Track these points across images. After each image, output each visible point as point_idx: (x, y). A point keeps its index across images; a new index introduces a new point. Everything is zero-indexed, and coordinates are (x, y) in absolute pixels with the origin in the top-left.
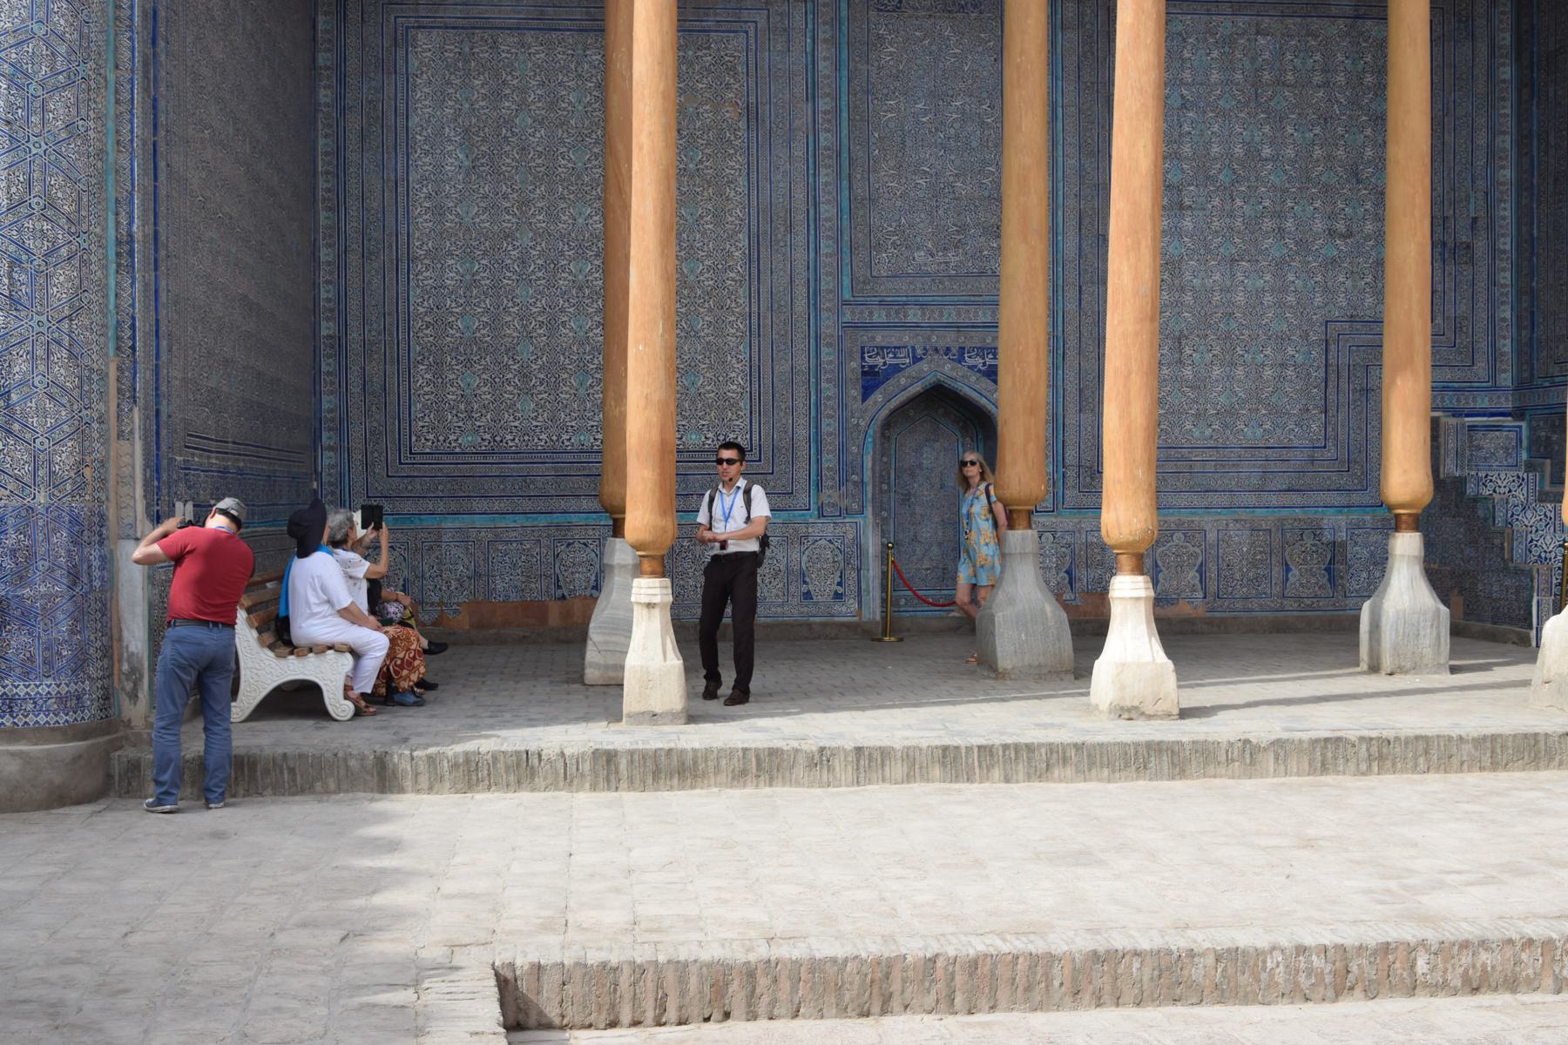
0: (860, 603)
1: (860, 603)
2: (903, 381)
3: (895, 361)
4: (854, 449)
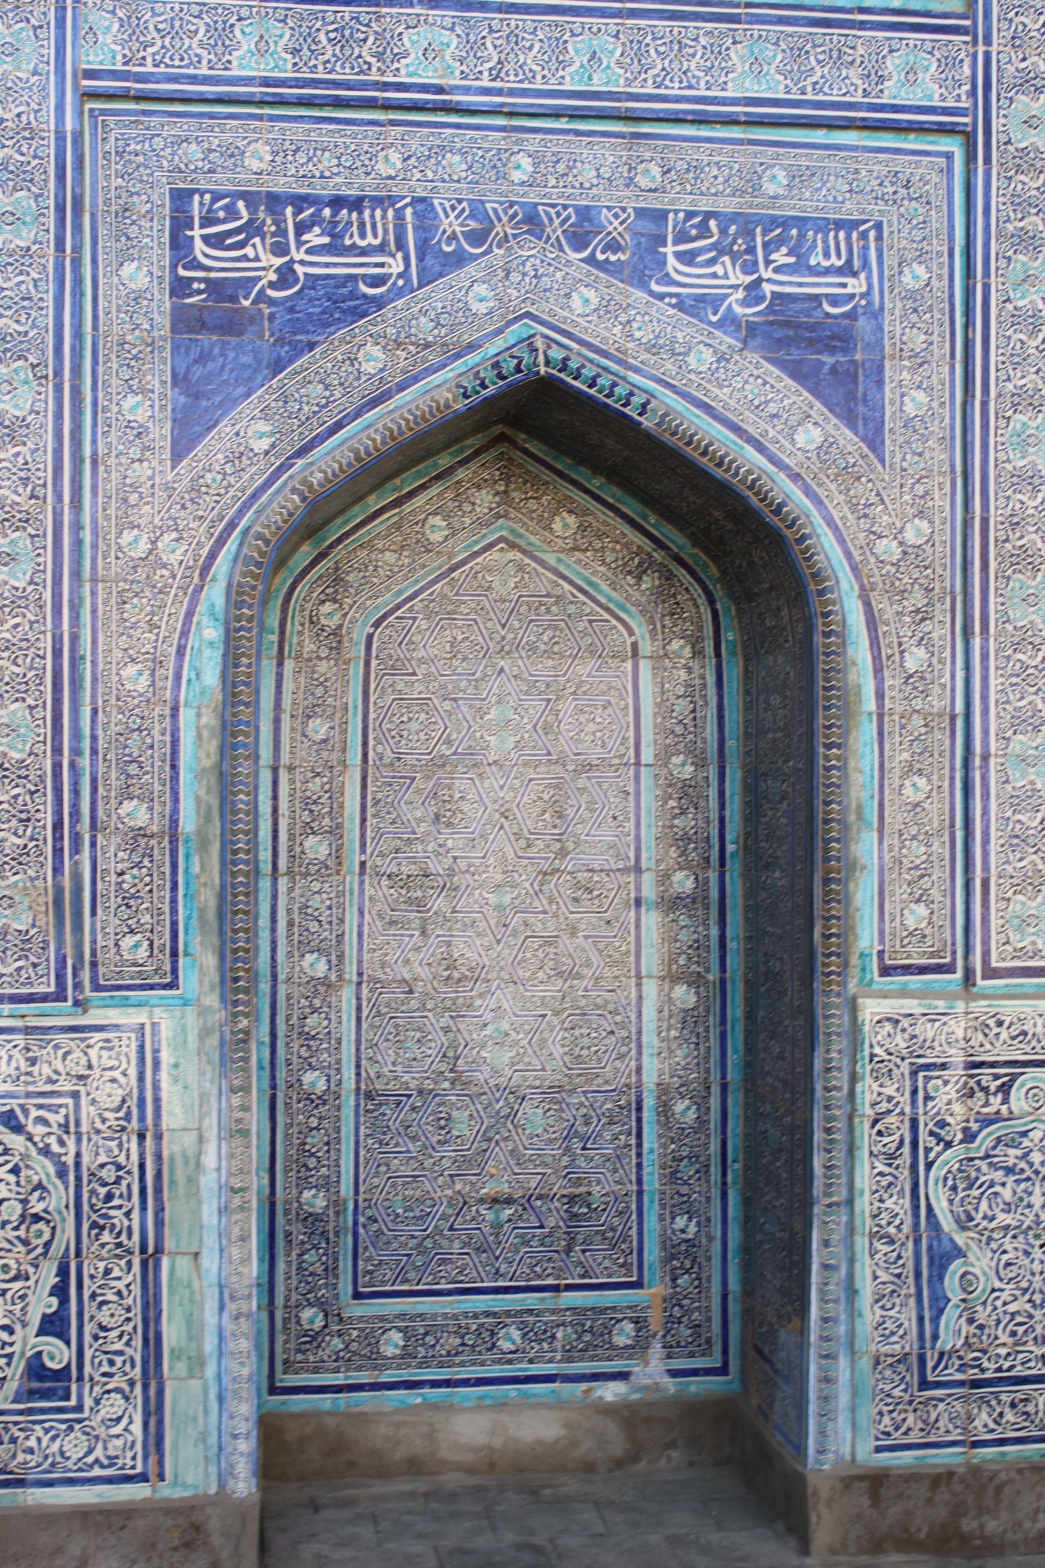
0: (154, 1412)
1: (154, 1412)
2: (373, 359)
3: (339, 266)
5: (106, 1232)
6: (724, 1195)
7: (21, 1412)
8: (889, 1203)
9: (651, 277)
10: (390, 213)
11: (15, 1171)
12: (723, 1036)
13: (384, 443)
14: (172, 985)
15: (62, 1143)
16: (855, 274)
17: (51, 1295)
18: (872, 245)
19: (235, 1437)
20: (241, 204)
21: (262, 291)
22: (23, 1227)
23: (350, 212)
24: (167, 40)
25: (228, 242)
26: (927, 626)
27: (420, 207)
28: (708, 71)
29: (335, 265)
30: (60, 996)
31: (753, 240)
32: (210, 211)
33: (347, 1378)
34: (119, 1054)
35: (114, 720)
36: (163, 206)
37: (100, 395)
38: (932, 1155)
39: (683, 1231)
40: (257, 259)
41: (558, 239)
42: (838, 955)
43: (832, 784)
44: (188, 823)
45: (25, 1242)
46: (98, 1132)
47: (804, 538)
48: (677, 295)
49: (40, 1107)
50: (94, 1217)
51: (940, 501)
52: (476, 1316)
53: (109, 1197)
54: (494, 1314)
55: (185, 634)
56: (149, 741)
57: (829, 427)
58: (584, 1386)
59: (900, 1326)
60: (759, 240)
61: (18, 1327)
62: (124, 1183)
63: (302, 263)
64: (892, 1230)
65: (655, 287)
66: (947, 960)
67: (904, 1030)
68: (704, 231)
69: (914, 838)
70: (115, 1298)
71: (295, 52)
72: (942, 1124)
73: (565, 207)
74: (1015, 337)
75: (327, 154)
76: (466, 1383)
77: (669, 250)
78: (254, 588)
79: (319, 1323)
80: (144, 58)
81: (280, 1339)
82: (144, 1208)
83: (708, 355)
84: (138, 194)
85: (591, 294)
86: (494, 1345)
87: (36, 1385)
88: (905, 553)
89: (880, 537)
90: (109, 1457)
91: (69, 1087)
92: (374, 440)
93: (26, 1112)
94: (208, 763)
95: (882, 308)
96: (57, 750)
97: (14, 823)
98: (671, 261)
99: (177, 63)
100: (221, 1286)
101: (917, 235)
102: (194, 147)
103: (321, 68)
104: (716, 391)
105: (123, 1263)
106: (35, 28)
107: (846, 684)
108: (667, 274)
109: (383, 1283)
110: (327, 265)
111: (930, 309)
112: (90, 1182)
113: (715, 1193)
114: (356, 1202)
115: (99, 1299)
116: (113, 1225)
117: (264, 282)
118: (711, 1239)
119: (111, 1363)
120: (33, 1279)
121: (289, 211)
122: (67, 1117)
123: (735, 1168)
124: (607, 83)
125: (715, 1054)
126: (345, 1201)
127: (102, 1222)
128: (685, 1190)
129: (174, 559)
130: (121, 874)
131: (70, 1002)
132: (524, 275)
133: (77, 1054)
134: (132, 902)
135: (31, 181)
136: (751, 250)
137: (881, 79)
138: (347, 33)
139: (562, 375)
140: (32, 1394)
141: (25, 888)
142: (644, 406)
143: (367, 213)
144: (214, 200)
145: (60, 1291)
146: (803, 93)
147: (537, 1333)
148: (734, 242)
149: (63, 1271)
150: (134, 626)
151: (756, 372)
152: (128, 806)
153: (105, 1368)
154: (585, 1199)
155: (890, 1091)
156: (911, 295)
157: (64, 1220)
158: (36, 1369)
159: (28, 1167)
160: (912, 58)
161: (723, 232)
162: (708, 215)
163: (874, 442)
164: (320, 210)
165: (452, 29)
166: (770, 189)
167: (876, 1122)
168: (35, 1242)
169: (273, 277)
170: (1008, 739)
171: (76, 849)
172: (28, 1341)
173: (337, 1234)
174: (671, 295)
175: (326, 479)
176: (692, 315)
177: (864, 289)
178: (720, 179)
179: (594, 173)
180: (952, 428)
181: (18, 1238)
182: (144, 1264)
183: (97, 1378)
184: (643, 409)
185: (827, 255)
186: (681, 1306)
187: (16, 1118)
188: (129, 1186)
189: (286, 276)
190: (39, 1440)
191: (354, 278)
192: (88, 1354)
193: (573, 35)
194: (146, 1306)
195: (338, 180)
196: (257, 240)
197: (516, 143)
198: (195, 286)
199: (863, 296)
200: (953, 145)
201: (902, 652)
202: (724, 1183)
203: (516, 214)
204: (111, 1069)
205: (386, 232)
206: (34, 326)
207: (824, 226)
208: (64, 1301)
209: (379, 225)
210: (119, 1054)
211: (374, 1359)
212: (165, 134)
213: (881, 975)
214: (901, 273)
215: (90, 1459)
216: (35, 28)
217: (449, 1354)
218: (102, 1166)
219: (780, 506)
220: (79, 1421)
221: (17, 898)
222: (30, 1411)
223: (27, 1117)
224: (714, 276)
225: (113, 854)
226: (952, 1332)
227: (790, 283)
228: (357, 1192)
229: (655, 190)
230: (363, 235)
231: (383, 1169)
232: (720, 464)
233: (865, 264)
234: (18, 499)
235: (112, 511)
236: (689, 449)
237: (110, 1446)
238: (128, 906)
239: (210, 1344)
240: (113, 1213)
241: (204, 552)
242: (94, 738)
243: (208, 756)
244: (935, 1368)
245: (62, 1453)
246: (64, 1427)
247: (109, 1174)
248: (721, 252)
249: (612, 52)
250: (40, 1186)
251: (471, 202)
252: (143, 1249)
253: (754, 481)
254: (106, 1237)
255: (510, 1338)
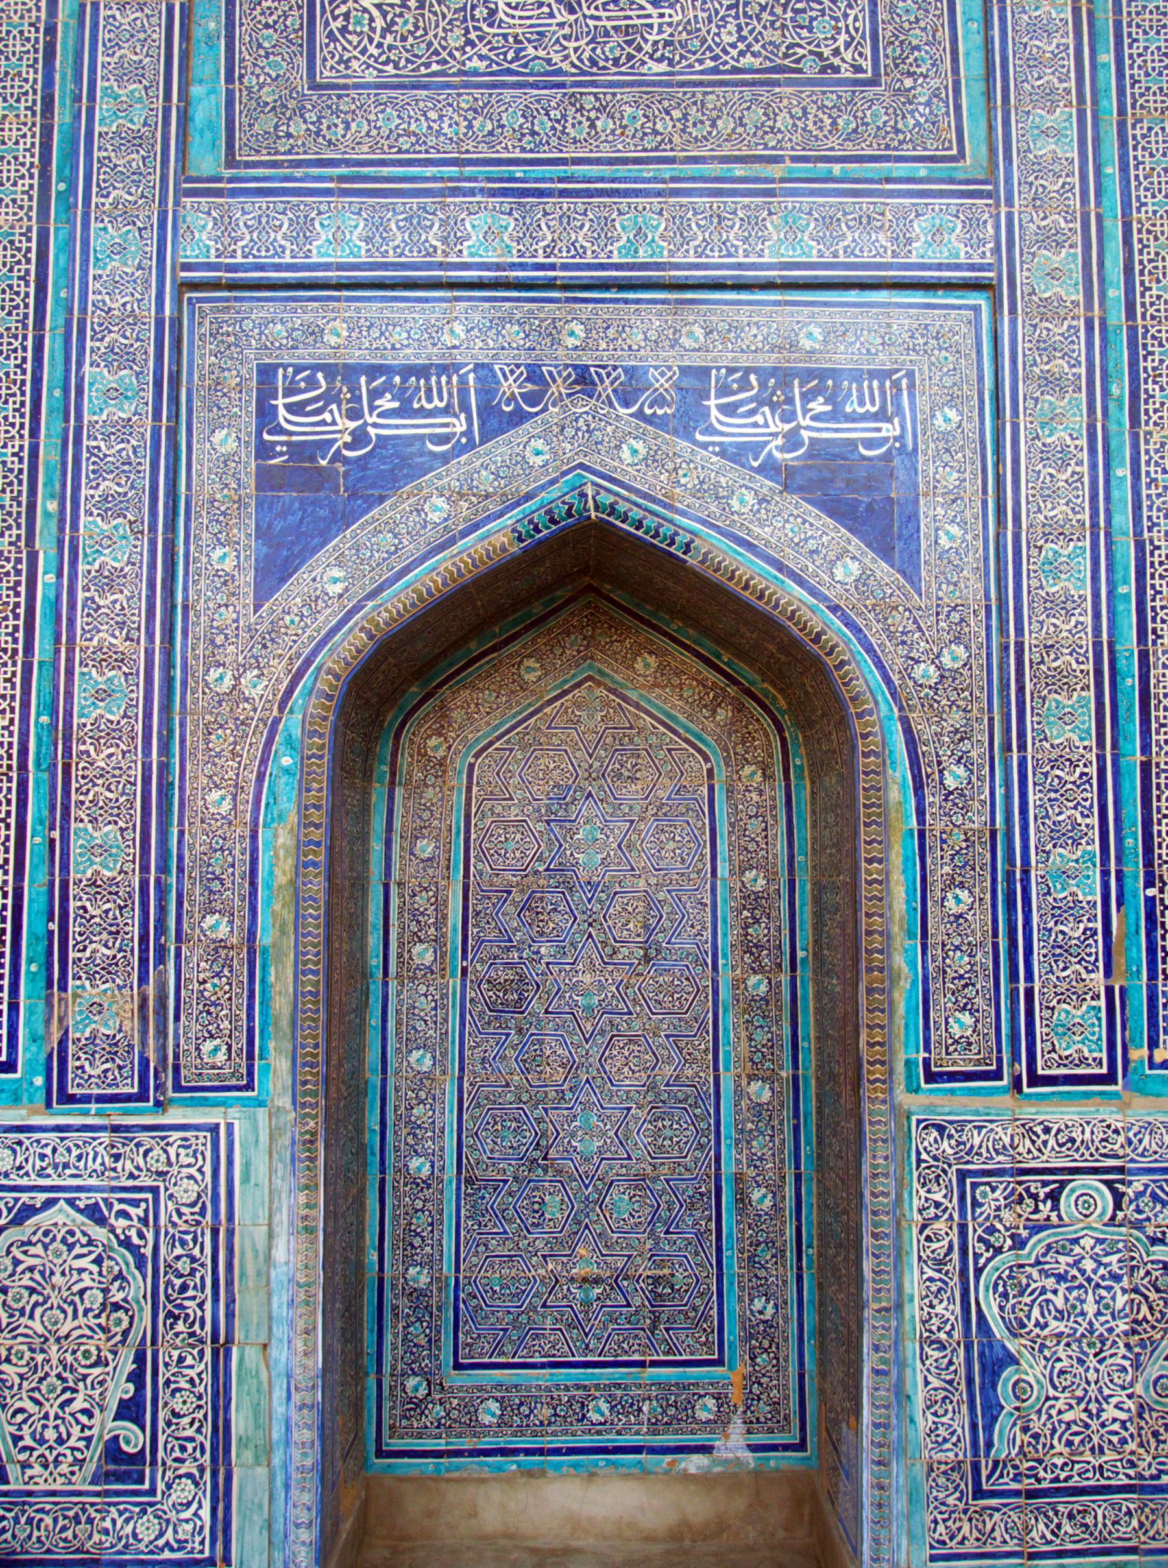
0: (222, 1498)
1: (222, 1498)
2: (438, 509)
3: (405, 427)
4: (218, 801)
5: (181, 1322)
6: (800, 1278)
7: (98, 1494)
8: (939, 1309)
9: (695, 429)
10: (455, 378)
11: (98, 1261)
12: (796, 1128)
13: (445, 584)
14: (249, 1087)
15: (141, 1235)
16: (889, 420)
17: (128, 1381)
18: (905, 393)
19: (297, 1526)
20: (320, 375)
21: (338, 451)
22: (104, 1315)
23: (418, 381)
24: (255, 235)
25: (308, 409)
26: (966, 746)
27: (483, 373)
28: (745, 240)
29: (404, 426)
30: (142, 1096)
31: (792, 391)
32: (292, 382)
33: (447, 1444)
34: (195, 1152)
35: (197, 841)
36: (251, 379)
37: (192, 548)
38: (982, 1261)
39: (761, 1312)
40: (334, 423)
41: (608, 396)
42: (883, 1063)
43: (875, 897)
44: (265, 937)
45: (105, 1330)
46: (174, 1225)
47: (842, 663)
48: (720, 444)
49: (121, 1201)
50: (170, 1307)
51: (976, 626)
52: (567, 1388)
53: (184, 1288)
54: (585, 1388)
55: (264, 761)
56: (230, 859)
57: (867, 561)
58: (668, 1458)
59: (952, 1433)
60: (797, 391)
61: (97, 1411)
62: (198, 1275)
63: (375, 425)
64: (943, 1336)
65: (699, 437)
66: (994, 1067)
67: (950, 1137)
68: (745, 385)
69: (957, 948)
70: (188, 1386)
71: (368, 240)
72: (991, 1230)
73: (615, 368)
74: (1044, 472)
75: (398, 329)
76: (557, 1452)
77: (712, 403)
78: (325, 719)
79: (422, 1392)
80: (235, 251)
81: (387, 1405)
82: (216, 1300)
83: (750, 498)
84: (229, 370)
85: (639, 446)
86: (584, 1416)
87: (111, 1467)
88: (942, 676)
89: (917, 662)
90: (178, 1541)
91: (149, 1182)
92: (435, 582)
93: (110, 1206)
94: (282, 879)
95: (915, 449)
96: (145, 868)
97: (105, 936)
98: (714, 412)
99: (263, 254)
100: (289, 1376)
101: (947, 381)
102: (279, 326)
103: (391, 252)
104: (758, 530)
105: (195, 1352)
106: (140, 229)
107: (887, 802)
108: (711, 425)
109: (481, 1355)
110: (397, 427)
111: (962, 447)
112: (166, 1273)
113: (791, 1277)
114: (457, 1279)
115: (173, 1386)
116: (187, 1315)
117: (340, 443)
118: (786, 1320)
119: (183, 1449)
120: (112, 1365)
121: (363, 379)
122: (146, 1211)
123: (810, 1252)
124: (651, 256)
125: (789, 1145)
126: (447, 1278)
127: (177, 1312)
128: (762, 1273)
129: (255, 693)
130: (205, 982)
131: (151, 1103)
132: (578, 429)
133: (157, 1151)
134: (212, 1009)
135: (134, 361)
136: (790, 401)
137: (909, 241)
138: (415, 221)
139: (611, 519)
140: (109, 1477)
141: (114, 996)
142: (688, 545)
143: (434, 379)
144: (296, 373)
145: (137, 1378)
146: (835, 256)
147: (624, 1407)
148: (773, 394)
149: (140, 1358)
150: (219, 755)
151: (795, 512)
152: (210, 920)
153: (177, 1454)
154: (669, 1281)
155: (938, 1197)
156: (944, 436)
157: (141, 1309)
158: (113, 1451)
159: (110, 1258)
160: (937, 222)
161: (763, 385)
162: (748, 371)
163: (910, 572)
164: (392, 379)
165: (510, 214)
166: (807, 344)
167: (924, 1227)
168: (114, 1330)
169: (348, 439)
170: (1048, 853)
171: (161, 959)
172: (106, 1425)
173: (439, 1309)
174: (714, 444)
175: (392, 618)
176: (735, 462)
177: (898, 433)
178: (760, 337)
179: (641, 336)
180: (986, 559)
181: (99, 1325)
182: (215, 1353)
183: (169, 1463)
184: (687, 548)
185: (861, 403)
186: (760, 1384)
187: (101, 1211)
188: (202, 1278)
189: (359, 438)
190: (114, 1521)
191: (421, 438)
192: (161, 1439)
193: (620, 214)
194: (216, 1394)
195: (408, 351)
196: (334, 407)
197: (569, 313)
198: (278, 448)
199: (896, 439)
200: (980, 300)
201: (941, 772)
202: (800, 1268)
203: (569, 375)
204: (189, 1165)
205: (450, 394)
206: (132, 487)
207: (857, 376)
208: (140, 1387)
209: (445, 390)
210: (195, 1152)
211: (473, 1426)
212: (253, 317)
213: (926, 1082)
214: (933, 416)
215: (161, 1542)
216: (140, 229)
217: (542, 1423)
218: (178, 1258)
219: (819, 635)
220: (151, 1504)
221: (106, 1005)
222: (107, 1493)
223: (110, 1210)
224: (755, 425)
225: (197, 964)
226: (1006, 1438)
227: (827, 429)
228: (457, 1270)
229: (699, 350)
230: (430, 400)
231: (482, 1248)
232: (761, 597)
233: (899, 410)
234: (114, 641)
235: (200, 651)
236: (731, 584)
237: (180, 1530)
238: (209, 1013)
239: (277, 1433)
240: (187, 1303)
241: (283, 687)
242: (180, 858)
243: (284, 873)
244: (989, 1477)
245: (135, 1535)
246: (137, 1509)
247: (184, 1266)
248: (761, 404)
249: (656, 228)
250: (120, 1276)
251: (528, 366)
252: (215, 1338)
253: (793, 612)
254: (180, 1326)
255: (598, 1411)
